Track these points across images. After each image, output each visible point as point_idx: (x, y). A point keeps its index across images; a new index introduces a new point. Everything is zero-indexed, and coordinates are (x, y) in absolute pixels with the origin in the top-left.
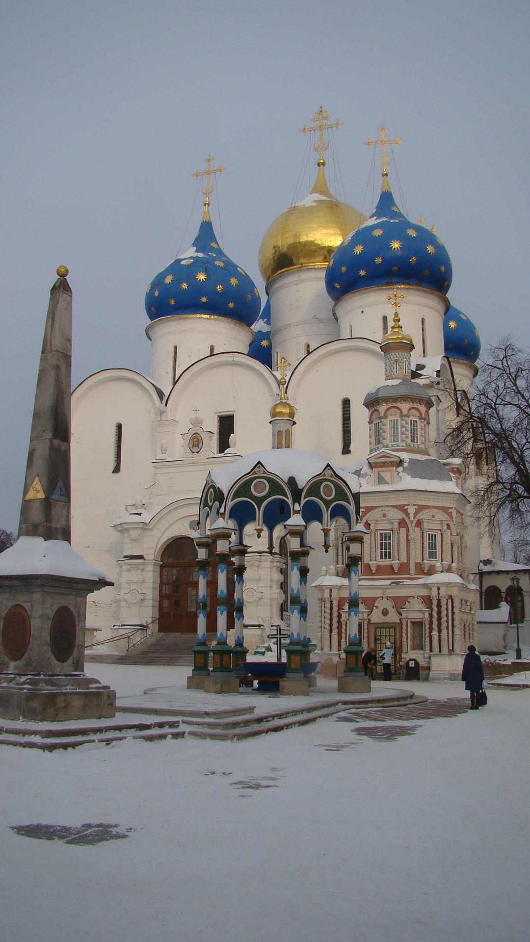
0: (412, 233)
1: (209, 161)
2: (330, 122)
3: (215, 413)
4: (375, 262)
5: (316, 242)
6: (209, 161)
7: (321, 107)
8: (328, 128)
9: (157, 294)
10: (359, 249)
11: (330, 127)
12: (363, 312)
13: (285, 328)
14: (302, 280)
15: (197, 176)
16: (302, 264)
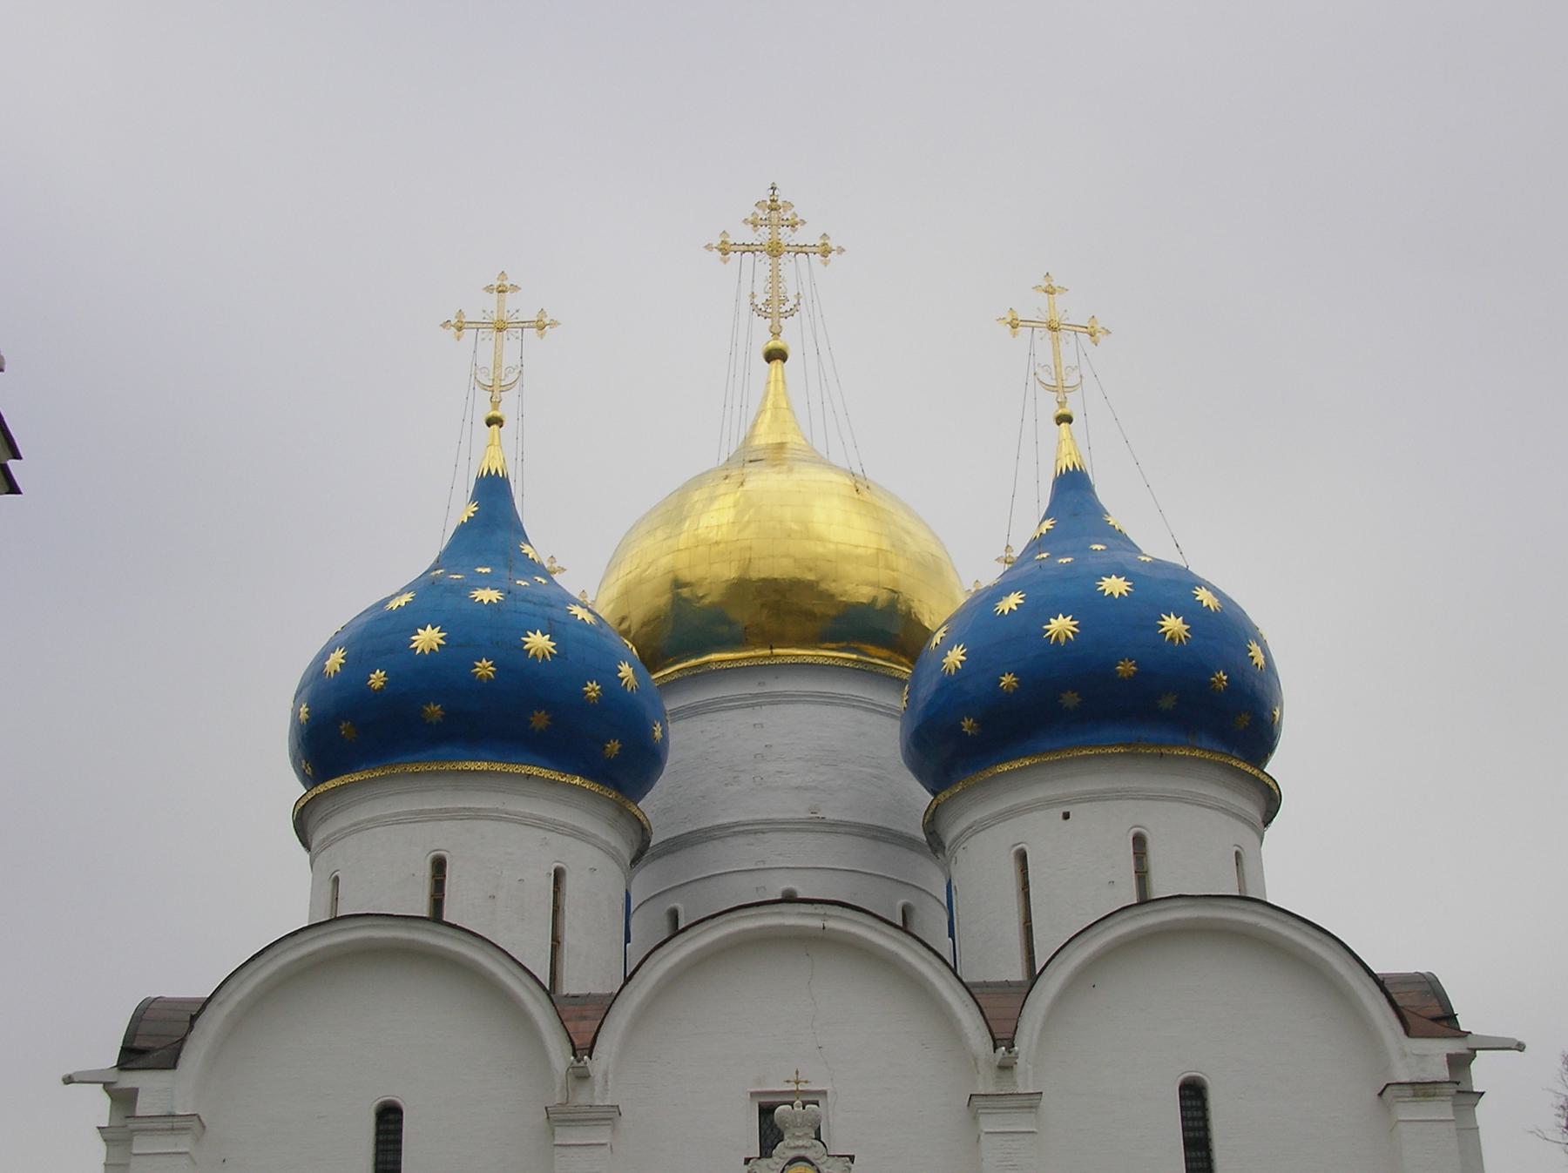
0: (1204, 596)
2: (803, 236)
3: (752, 1094)
4: (1118, 672)
5: (823, 586)
7: (773, 188)
9: (377, 679)
10: (1061, 625)
11: (801, 250)
12: (1066, 816)
13: (713, 838)
14: (770, 695)
15: (460, 329)
16: (771, 648)
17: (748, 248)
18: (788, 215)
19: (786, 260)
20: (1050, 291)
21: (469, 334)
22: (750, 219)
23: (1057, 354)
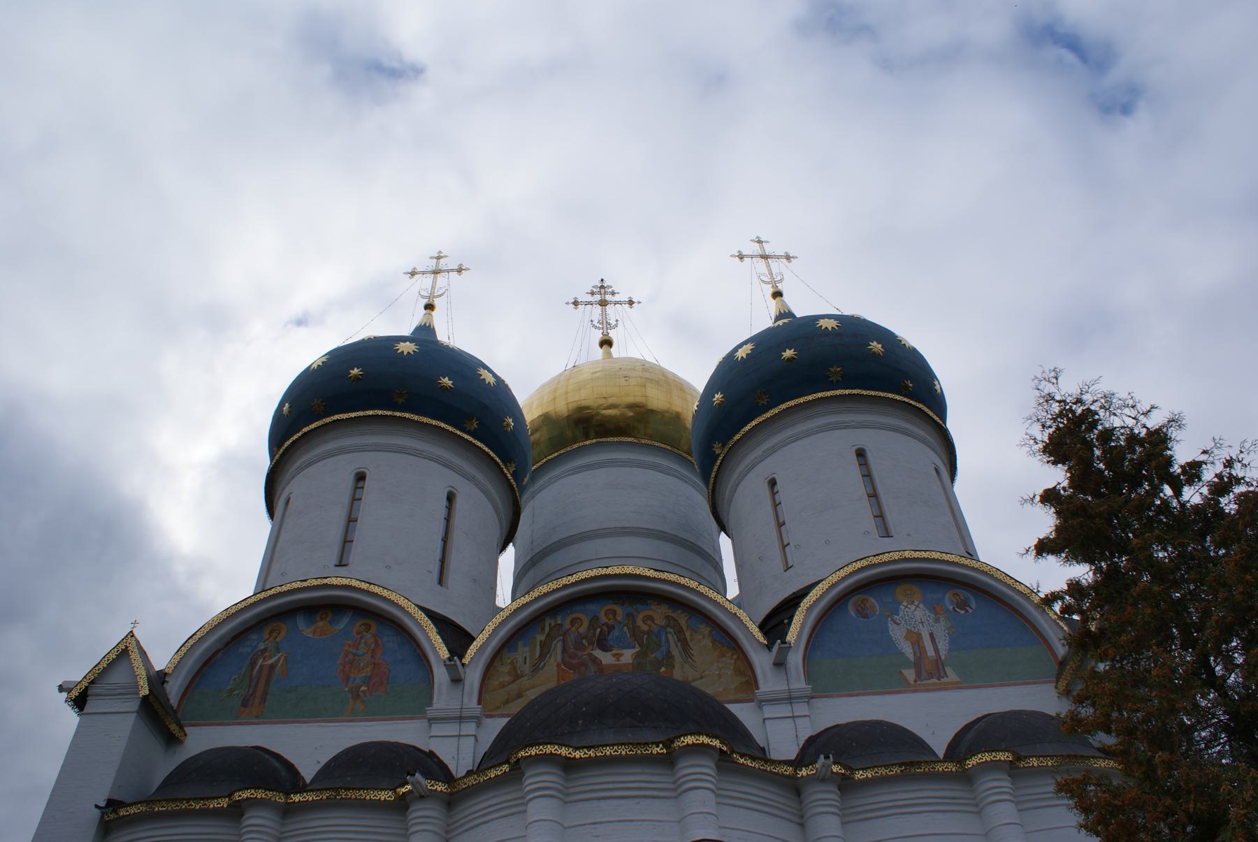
1: (438, 258)
2: (616, 298)
6: (438, 258)
8: (615, 304)
11: (616, 303)
17: (590, 303)
18: (610, 290)
19: (610, 309)
20: (760, 242)
21: (417, 276)
22: (590, 292)
23: (768, 266)
